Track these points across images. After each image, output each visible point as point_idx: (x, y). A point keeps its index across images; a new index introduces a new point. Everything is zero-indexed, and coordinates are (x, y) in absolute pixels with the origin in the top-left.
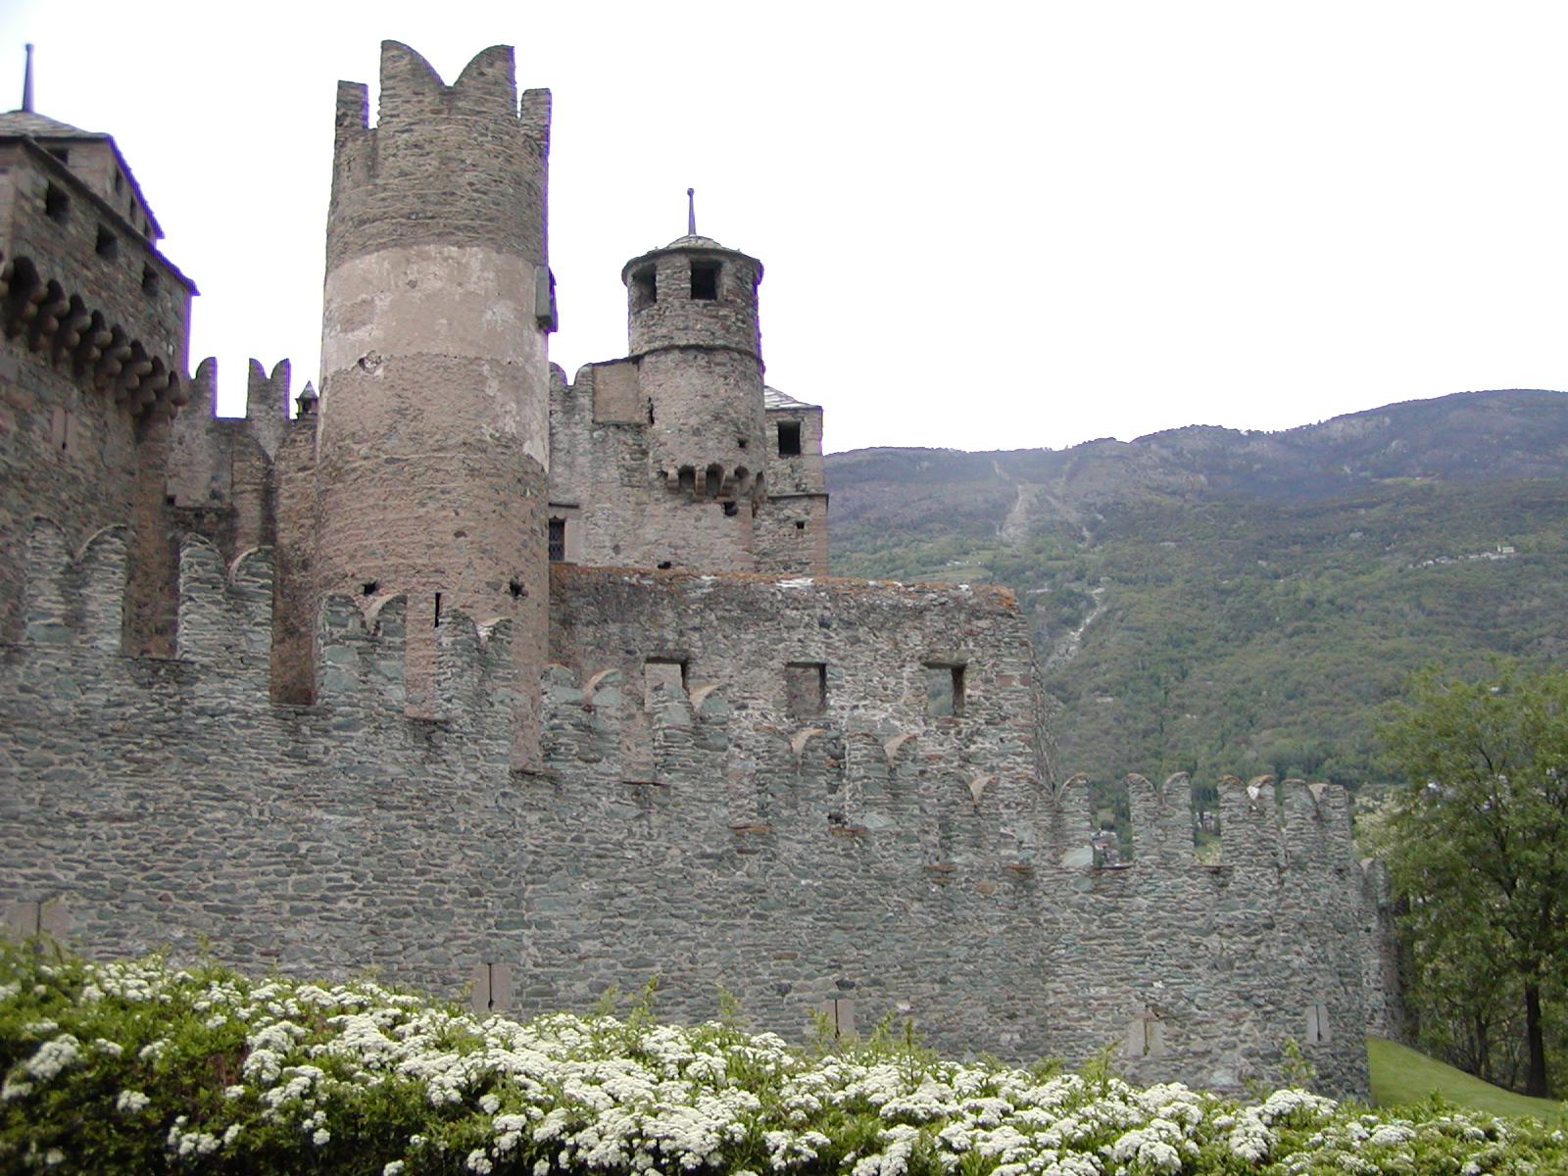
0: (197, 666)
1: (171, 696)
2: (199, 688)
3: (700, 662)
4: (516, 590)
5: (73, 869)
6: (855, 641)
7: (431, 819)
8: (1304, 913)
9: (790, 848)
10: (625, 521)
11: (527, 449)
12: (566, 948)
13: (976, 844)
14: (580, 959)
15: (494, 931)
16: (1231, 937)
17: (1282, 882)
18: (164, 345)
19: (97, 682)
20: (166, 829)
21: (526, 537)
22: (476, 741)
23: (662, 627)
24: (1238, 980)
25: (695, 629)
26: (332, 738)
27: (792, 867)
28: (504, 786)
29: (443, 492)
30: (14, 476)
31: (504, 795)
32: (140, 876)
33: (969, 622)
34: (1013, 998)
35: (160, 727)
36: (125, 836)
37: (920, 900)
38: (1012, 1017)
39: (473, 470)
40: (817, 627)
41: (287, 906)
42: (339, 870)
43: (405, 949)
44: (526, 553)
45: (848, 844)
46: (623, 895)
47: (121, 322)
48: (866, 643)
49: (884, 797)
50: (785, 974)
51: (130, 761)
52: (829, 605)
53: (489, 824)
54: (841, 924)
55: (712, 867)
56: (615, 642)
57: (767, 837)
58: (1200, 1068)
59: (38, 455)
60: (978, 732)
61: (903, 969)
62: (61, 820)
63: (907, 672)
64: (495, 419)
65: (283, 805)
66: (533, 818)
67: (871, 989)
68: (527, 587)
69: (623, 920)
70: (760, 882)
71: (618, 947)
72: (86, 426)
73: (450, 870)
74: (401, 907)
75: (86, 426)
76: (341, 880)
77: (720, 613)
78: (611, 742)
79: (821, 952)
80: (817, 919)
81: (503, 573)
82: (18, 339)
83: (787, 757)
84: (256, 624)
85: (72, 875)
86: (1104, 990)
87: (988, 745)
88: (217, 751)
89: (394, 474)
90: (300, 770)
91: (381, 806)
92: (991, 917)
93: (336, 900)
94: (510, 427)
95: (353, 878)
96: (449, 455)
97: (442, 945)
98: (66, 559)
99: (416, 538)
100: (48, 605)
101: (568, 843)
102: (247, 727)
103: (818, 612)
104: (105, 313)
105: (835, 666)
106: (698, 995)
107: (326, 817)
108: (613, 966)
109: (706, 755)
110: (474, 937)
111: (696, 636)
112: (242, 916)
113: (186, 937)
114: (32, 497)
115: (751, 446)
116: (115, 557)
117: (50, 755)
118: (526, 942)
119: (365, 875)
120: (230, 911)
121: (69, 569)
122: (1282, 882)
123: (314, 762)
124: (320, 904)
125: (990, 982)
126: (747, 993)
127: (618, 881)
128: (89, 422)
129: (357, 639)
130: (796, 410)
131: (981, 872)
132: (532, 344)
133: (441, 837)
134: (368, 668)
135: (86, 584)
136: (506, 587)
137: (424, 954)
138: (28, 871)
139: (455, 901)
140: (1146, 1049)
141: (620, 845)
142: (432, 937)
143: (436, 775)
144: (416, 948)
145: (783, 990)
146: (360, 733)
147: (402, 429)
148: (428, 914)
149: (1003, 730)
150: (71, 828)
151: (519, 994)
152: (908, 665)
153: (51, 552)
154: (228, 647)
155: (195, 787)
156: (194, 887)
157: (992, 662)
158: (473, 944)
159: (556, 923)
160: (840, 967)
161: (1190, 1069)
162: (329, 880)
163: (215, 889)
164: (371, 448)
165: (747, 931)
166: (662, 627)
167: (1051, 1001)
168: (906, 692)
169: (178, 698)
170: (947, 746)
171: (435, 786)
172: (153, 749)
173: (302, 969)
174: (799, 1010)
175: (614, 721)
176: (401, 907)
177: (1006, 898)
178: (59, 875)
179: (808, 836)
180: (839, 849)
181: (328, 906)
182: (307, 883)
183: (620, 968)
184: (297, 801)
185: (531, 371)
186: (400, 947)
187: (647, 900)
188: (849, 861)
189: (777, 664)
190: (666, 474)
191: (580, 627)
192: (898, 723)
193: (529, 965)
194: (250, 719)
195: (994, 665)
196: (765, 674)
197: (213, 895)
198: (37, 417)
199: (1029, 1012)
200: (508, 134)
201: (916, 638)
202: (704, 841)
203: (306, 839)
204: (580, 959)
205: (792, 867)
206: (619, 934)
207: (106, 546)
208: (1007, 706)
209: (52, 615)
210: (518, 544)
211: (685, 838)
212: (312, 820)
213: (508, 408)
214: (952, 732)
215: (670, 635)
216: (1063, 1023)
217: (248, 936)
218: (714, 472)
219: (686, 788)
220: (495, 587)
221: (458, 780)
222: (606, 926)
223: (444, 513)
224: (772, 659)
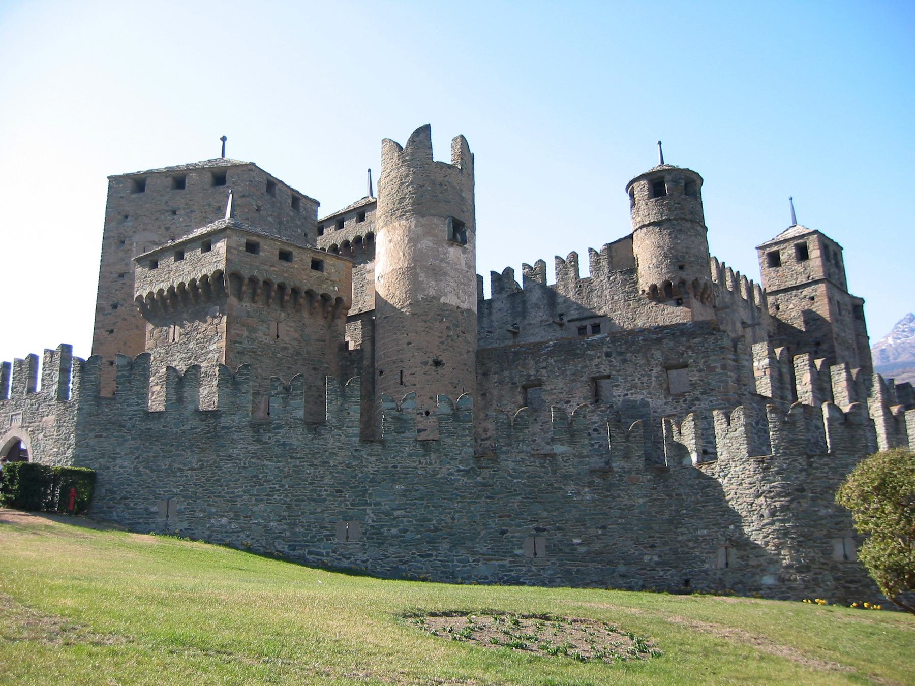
1: (212, 424)
2: (223, 420)
3: (546, 383)
4: (437, 363)
5: (179, 488)
6: (625, 361)
7: (315, 462)
8: (831, 481)
9: (508, 464)
10: (628, 318)
11: (442, 300)
12: (388, 514)
13: (627, 456)
14: (395, 519)
15: (350, 507)
16: (772, 498)
17: (810, 465)
18: (332, 288)
19: (187, 422)
20: (210, 472)
21: (443, 340)
22: (340, 429)
23: (528, 369)
24: (777, 524)
25: (544, 368)
26: (272, 433)
27: (510, 475)
28: (356, 447)
29: (402, 327)
30: (250, 352)
31: (356, 450)
32: (201, 489)
33: (688, 341)
34: (653, 537)
35: (209, 435)
36: (197, 476)
37: (589, 487)
38: (653, 546)
40: (605, 358)
41: (254, 498)
42: (274, 484)
43: (303, 513)
44: (444, 347)
45: (542, 461)
46: (418, 490)
47: (298, 284)
48: (631, 361)
49: (565, 437)
50: (504, 525)
51: (198, 448)
52: (610, 345)
53: (347, 462)
54: (539, 499)
55: (463, 476)
56: (507, 379)
57: (495, 460)
58: (754, 574)
59: (262, 341)
60: (698, 399)
61: (577, 522)
62: (176, 472)
63: (654, 373)
64: (424, 289)
65: (253, 460)
66: (374, 459)
67: (556, 532)
68: (444, 362)
69: (416, 501)
70: (491, 482)
71: (414, 513)
72: (291, 327)
73: (325, 482)
74: (301, 497)
75: (291, 327)
76: (275, 488)
77: (555, 358)
78: (410, 424)
79: (526, 514)
80: (524, 498)
81: (429, 357)
82: (245, 300)
83: (505, 422)
84: (243, 393)
85: (179, 490)
86: (705, 531)
87: (702, 405)
88: (229, 442)
90: (259, 446)
91: (292, 458)
92: (638, 494)
93: (273, 496)
94: (432, 292)
95: (280, 487)
97: (321, 512)
98: (177, 379)
99: (393, 349)
101: (390, 469)
102: (239, 432)
103: (605, 349)
104: (287, 282)
105: (615, 375)
106: (456, 534)
107: (270, 464)
108: (411, 521)
109: (460, 425)
110: (337, 509)
111: (544, 372)
112: (237, 503)
113: (217, 511)
114: (259, 358)
115: (686, 267)
116: (193, 376)
117: (173, 449)
118: (368, 511)
119: (285, 485)
120: (233, 500)
121: (178, 383)
122: (810, 465)
123: (265, 443)
124: (266, 498)
125: (636, 528)
126: (483, 533)
127: (414, 484)
128: (292, 324)
129: (282, 394)
130: (803, 236)
131: (630, 472)
132: (445, 254)
133: (321, 470)
134: (286, 403)
135: (183, 387)
136: (431, 362)
137: (311, 516)
138: (164, 490)
139: (327, 495)
140: (727, 564)
141: (415, 468)
142: (316, 509)
143: (318, 444)
144: (308, 514)
145: (503, 532)
146: (283, 430)
148: (314, 500)
149: (712, 396)
150: (178, 474)
151: (364, 533)
152: (655, 369)
153: (172, 378)
154: (233, 403)
155: (220, 456)
156: (220, 492)
157: (703, 360)
158: (337, 512)
159: (383, 504)
160: (537, 521)
161: (749, 575)
162: (270, 488)
163: (227, 493)
165: (483, 504)
166: (528, 369)
167: (680, 538)
168: (653, 383)
169: (214, 424)
170: (678, 409)
171: (318, 448)
172: (206, 443)
173: (259, 523)
174: (512, 542)
175: (411, 414)
176: (301, 497)
177: (649, 484)
178: (175, 490)
179: (518, 458)
180: (537, 464)
181: (270, 498)
182: (262, 488)
183: (414, 522)
184: (259, 459)
185: (444, 265)
186: (300, 513)
187: (428, 492)
188: (543, 470)
189: (584, 378)
190: (643, 291)
191: (491, 375)
192: (650, 400)
193: (370, 521)
195: (704, 362)
196: (579, 384)
197: (227, 496)
198: (260, 328)
199: (665, 544)
200: (427, 164)
201: (658, 354)
202: (459, 464)
203: (262, 473)
204: (395, 519)
205: (510, 475)
206: (414, 507)
207: (190, 373)
208: (714, 383)
210: (438, 344)
211: (449, 463)
212: (264, 465)
213: (431, 285)
214: (681, 401)
215: (532, 372)
216: (687, 550)
217: (239, 510)
218: (667, 284)
219: (449, 441)
220: (426, 363)
221: (330, 446)
222: (407, 504)
224: (582, 376)
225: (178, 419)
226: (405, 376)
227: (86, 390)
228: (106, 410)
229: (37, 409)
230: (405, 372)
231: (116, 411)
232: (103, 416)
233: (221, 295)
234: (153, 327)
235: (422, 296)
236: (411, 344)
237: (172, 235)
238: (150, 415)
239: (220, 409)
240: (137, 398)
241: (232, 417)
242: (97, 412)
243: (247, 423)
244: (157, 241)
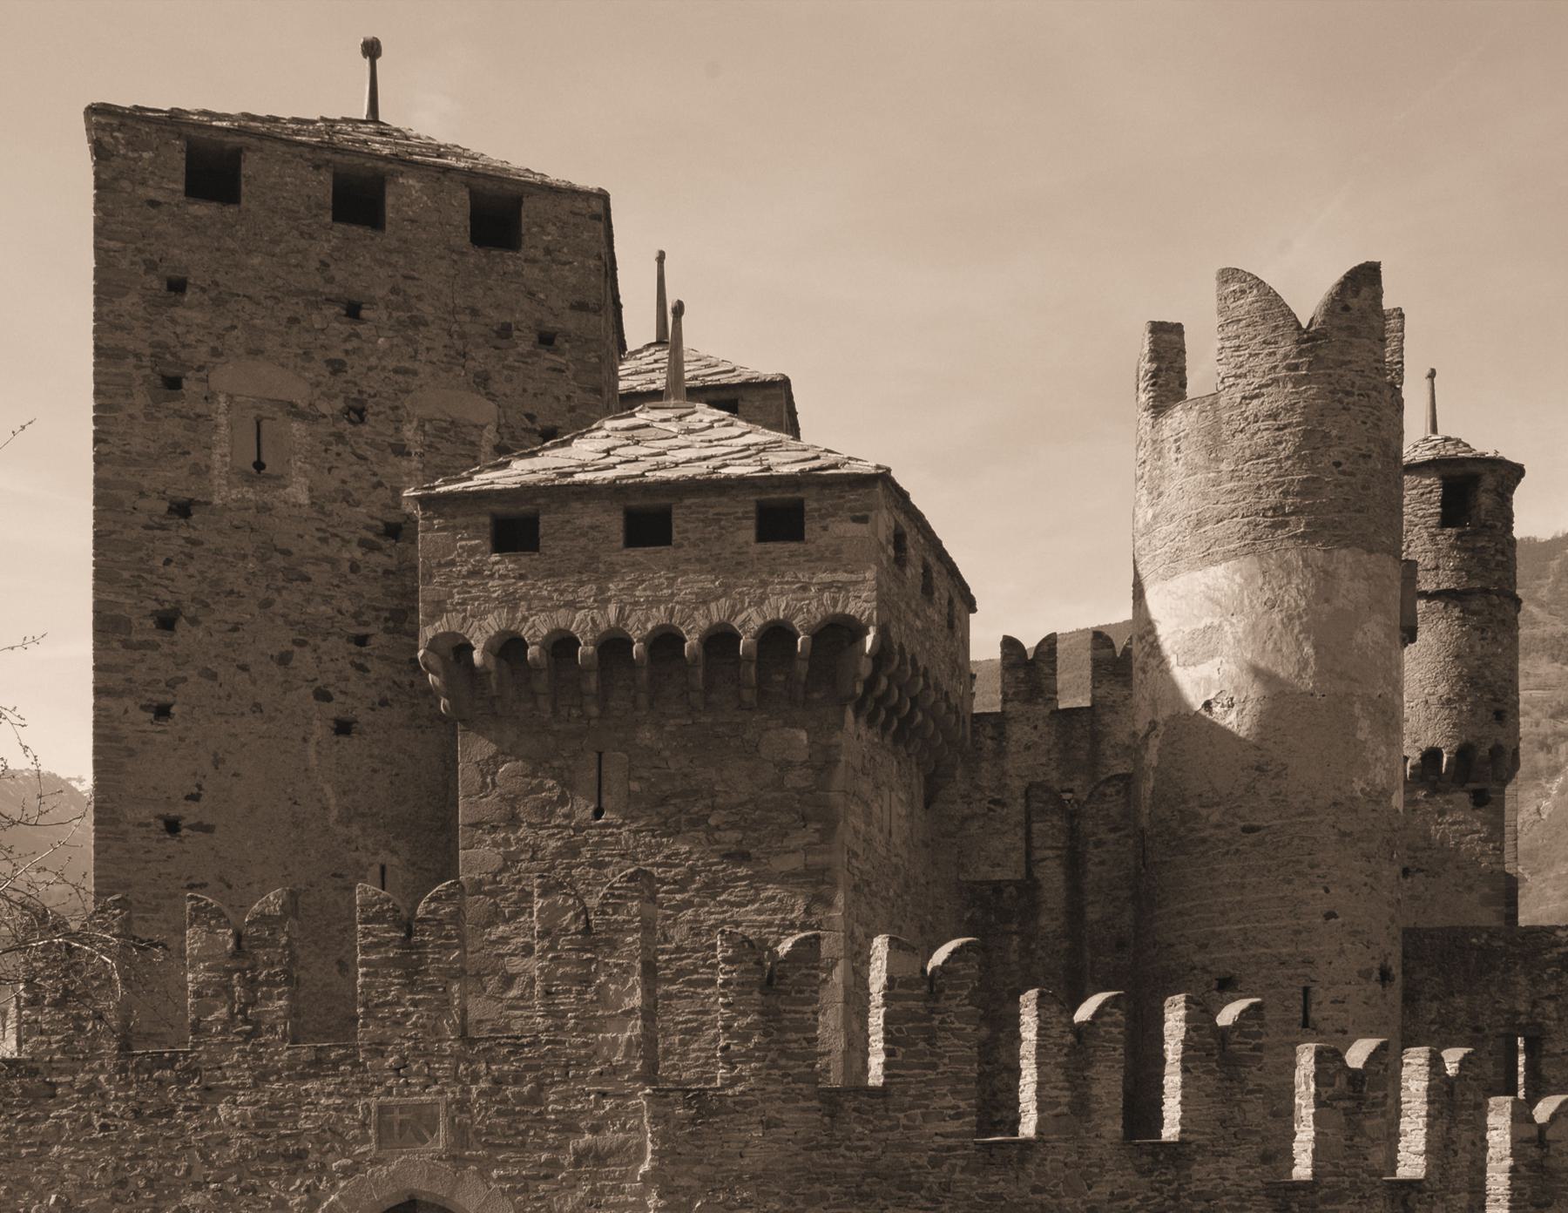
0: (1194, 1146)
1: (1169, 1183)
2: (1197, 1171)
29: (1312, 867)
39: (1344, 834)
89: (1254, 845)
96: (1317, 819)
100: (1055, 1093)
146: (1345, 1206)
147: (1258, 785)
164: (1224, 813)
169: (1175, 1185)
194: (1243, 1200)
209: (1059, 1104)
223: (1312, 891)
225: (1077, 1166)
226: (1320, 1003)
227: (791, 1056)
228: (859, 1129)
229: (535, 1098)
230: (1319, 994)
231: (890, 1135)
232: (848, 1148)
233: (816, 696)
234: (491, 749)
235: (1362, 784)
236: (1335, 916)
237: (355, 395)
238: (994, 1151)
239: (1191, 1138)
240: (954, 1092)
241: (1222, 1163)
242: (831, 1136)
243: (1260, 1185)
244: (302, 404)
